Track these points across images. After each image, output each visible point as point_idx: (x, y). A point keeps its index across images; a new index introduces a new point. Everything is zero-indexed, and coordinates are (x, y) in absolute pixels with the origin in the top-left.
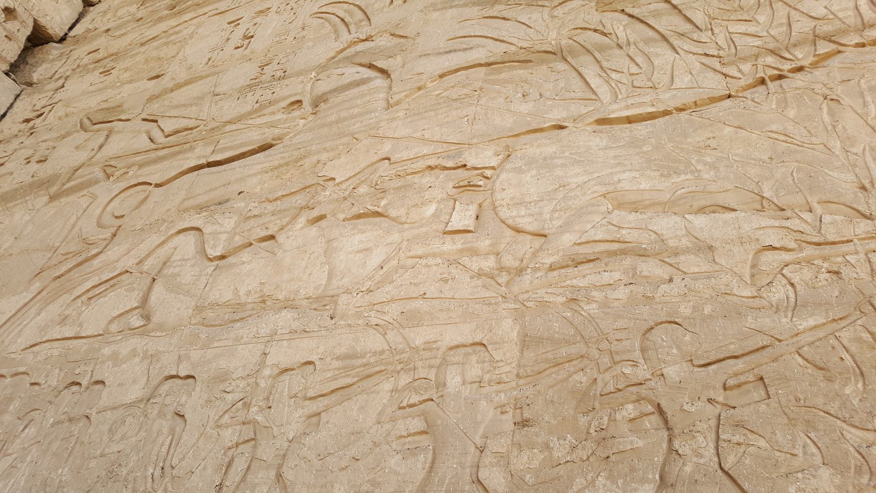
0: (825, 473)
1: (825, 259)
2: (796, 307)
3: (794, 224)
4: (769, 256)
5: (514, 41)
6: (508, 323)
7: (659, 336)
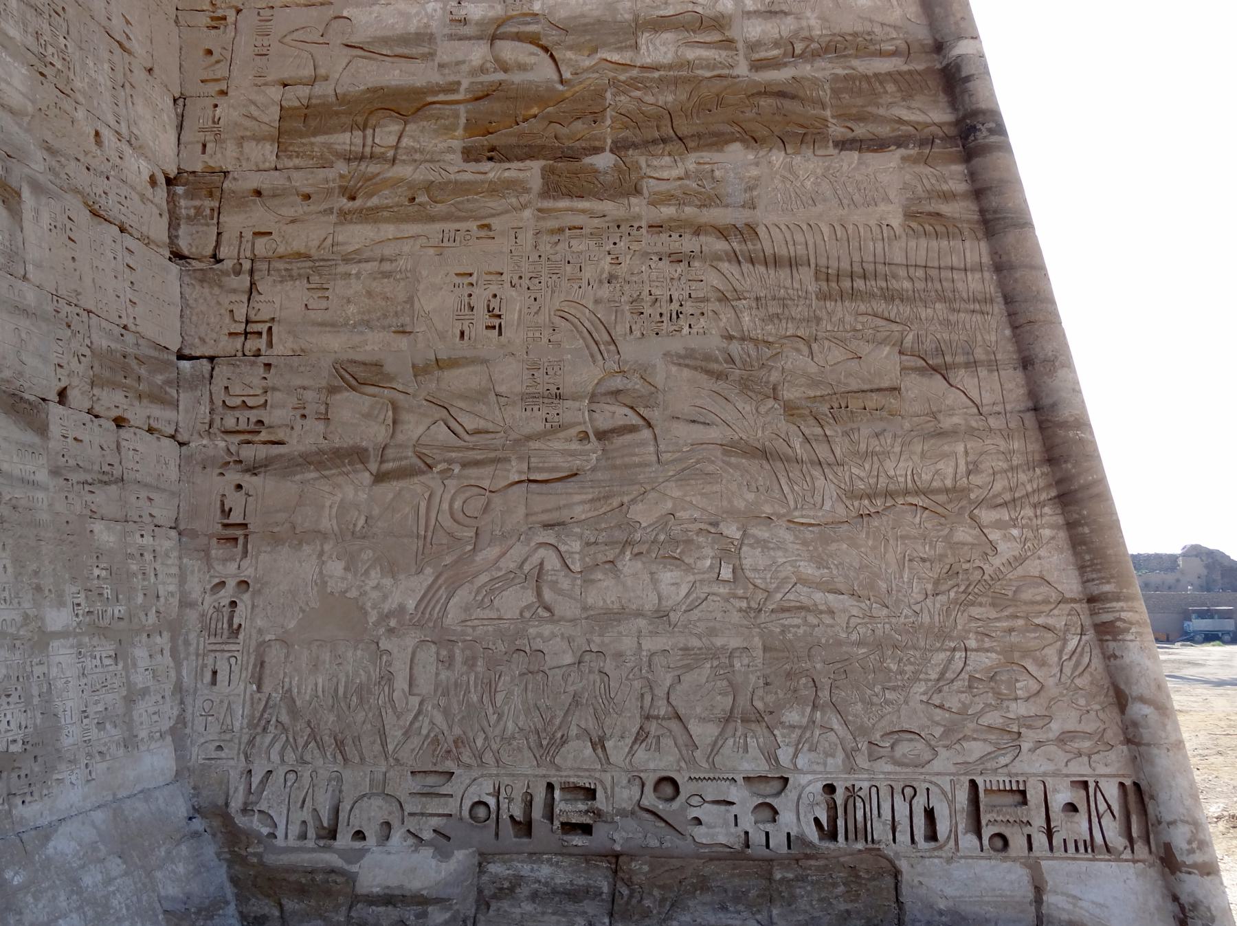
0: (859, 704)
1: (871, 624)
2: (860, 644)
3: (863, 605)
4: (853, 620)
5: (737, 429)
6: (757, 639)
7: (813, 652)
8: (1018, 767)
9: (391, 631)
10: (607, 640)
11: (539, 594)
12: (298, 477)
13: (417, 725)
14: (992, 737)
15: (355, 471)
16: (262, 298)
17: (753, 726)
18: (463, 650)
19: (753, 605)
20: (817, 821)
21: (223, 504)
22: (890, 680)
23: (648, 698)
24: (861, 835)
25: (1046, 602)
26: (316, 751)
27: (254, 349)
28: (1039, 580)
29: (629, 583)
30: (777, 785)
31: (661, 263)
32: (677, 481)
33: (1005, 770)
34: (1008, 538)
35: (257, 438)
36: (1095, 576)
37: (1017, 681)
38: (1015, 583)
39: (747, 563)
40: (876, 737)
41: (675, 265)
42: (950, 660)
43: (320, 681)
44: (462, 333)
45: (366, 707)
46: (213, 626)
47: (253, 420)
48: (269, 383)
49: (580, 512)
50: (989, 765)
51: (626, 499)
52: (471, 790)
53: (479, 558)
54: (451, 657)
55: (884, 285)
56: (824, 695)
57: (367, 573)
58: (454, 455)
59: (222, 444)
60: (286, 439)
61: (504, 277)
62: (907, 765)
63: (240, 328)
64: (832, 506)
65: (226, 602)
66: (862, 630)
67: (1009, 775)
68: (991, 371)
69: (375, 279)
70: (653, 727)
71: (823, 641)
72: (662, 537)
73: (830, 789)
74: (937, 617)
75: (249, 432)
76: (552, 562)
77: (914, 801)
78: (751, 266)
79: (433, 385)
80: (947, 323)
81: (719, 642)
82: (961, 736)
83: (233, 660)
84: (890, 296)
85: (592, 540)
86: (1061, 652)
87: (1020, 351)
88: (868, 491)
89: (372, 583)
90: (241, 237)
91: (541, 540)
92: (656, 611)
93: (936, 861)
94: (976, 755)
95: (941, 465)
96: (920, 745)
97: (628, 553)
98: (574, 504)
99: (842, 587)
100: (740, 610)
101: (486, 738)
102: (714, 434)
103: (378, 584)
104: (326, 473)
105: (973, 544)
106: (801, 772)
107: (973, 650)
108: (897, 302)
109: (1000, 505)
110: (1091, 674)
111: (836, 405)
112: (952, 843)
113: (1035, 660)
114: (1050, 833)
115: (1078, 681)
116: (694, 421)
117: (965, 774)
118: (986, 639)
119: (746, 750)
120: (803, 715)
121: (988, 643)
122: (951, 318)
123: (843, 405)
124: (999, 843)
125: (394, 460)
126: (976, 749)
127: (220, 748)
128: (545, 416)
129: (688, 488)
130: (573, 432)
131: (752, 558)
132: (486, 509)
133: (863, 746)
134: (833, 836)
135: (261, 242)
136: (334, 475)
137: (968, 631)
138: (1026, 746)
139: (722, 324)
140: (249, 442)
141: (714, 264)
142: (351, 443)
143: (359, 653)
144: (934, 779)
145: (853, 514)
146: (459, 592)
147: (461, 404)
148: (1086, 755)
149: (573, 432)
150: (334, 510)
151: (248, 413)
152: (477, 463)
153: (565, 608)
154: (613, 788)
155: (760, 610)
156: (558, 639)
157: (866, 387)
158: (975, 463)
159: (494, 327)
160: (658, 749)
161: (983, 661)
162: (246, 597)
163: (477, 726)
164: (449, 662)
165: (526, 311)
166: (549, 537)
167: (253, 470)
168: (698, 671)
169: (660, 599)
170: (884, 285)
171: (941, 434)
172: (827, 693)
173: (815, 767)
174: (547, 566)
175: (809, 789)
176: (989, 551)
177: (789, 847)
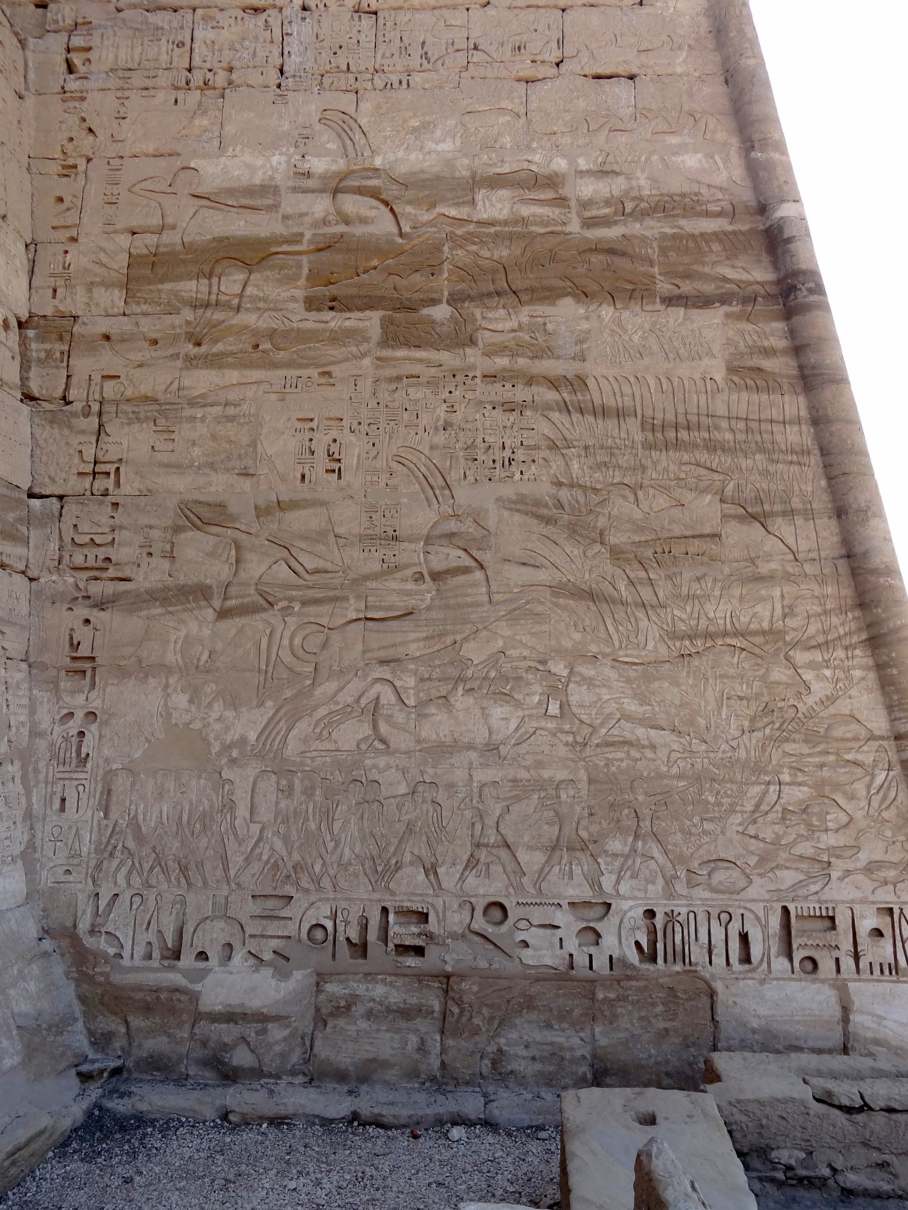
0: (679, 834)
2: (680, 777)
3: (683, 740)
4: (673, 755)
6: (582, 772)
7: (636, 784)
8: (827, 895)
9: (233, 761)
10: (439, 772)
11: (375, 727)
12: (144, 613)
13: (258, 851)
14: (804, 866)
15: (200, 608)
16: (110, 439)
17: (578, 854)
18: (302, 781)
19: (580, 739)
20: (637, 944)
21: (71, 638)
22: (707, 812)
23: (478, 827)
24: (679, 958)
25: (856, 739)
26: (161, 876)
27: (102, 488)
28: (850, 719)
29: (461, 716)
30: (601, 910)
31: (494, 412)
32: (507, 620)
33: (815, 897)
34: (820, 678)
35: (105, 575)
36: (902, 715)
37: (828, 813)
38: (828, 721)
39: (574, 699)
40: (695, 865)
41: (507, 413)
42: (765, 793)
43: (165, 809)
44: (303, 476)
45: (209, 834)
46: (62, 755)
47: (101, 557)
48: (117, 521)
49: (414, 649)
50: (800, 893)
51: (459, 638)
52: (309, 913)
53: (318, 692)
54: (291, 787)
55: (706, 435)
56: (646, 825)
57: (210, 705)
58: (294, 593)
59: (71, 580)
60: (133, 576)
61: (344, 423)
62: (723, 892)
63: (89, 468)
64: (655, 646)
65: (74, 732)
66: (681, 764)
67: (819, 901)
68: (807, 520)
69: (219, 423)
70: (483, 855)
71: (645, 774)
72: (493, 674)
73: (650, 914)
74: (753, 753)
75: (97, 569)
76: (388, 696)
77: (730, 926)
78: (580, 416)
79: (275, 526)
80: (765, 473)
81: (546, 774)
82: (774, 864)
83: (81, 788)
84: (712, 447)
85: (427, 676)
86: (869, 787)
87: (834, 500)
88: (689, 632)
89: (215, 715)
90: (90, 379)
91: (378, 676)
92: (487, 745)
93: (750, 982)
94: (789, 883)
95: (758, 608)
96: (735, 873)
97: (460, 689)
98: (409, 641)
99: (664, 724)
100: (567, 744)
101: (324, 864)
102: (543, 576)
103: (221, 716)
104: (171, 609)
105: (787, 684)
106: (623, 898)
107: (787, 784)
108: (719, 452)
109: (814, 647)
110: (897, 807)
111: (659, 550)
112: (765, 965)
113: (845, 793)
114: (857, 957)
115: (885, 814)
116: (524, 564)
117: (777, 901)
118: (799, 774)
119: (571, 877)
120: (626, 844)
121: (800, 778)
122: (770, 468)
123: (667, 550)
124: (809, 966)
125: (237, 597)
126: (789, 877)
127: (68, 872)
128: (382, 557)
129: (518, 627)
130: (409, 572)
131: (578, 695)
132: (325, 645)
133: (682, 874)
134: (653, 959)
135: (109, 385)
136: (178, 611)
137: (782, 766)
138: (835, 875)
139: (552, 472)
140: (96, 579)
141: (546, 413)
142: (196, 580)
143: (202, 782)
144: (748, 905)
145: (675, 654)
146: (298, 724)
147: (303, 545)
148: (891, 883)
149: (409, 572)
150: (179, 646)
151: (95, 551)
152: (316, 602)
153: (400, 740)
154: (444, 912)
155: (586, 744)
156: (393, 770)
157: (688, 533)
158: (790, 607)
159: (334, 471)
160: (488, 875)
161: (796, 794)
162: (94, 727)
163: (315, 853)
164: (289, 792)
165: (365, 455)
166: (385, 672)
167: (101, 605)
168: (526, 801)
169: (490, 733)
170: (706, 435)
171: (759, 579)
172: (648, 823)
173: (637, 894)
174: (383, 701)
175: (630, 914)
176: (803, 691)
177: (611, 969)
